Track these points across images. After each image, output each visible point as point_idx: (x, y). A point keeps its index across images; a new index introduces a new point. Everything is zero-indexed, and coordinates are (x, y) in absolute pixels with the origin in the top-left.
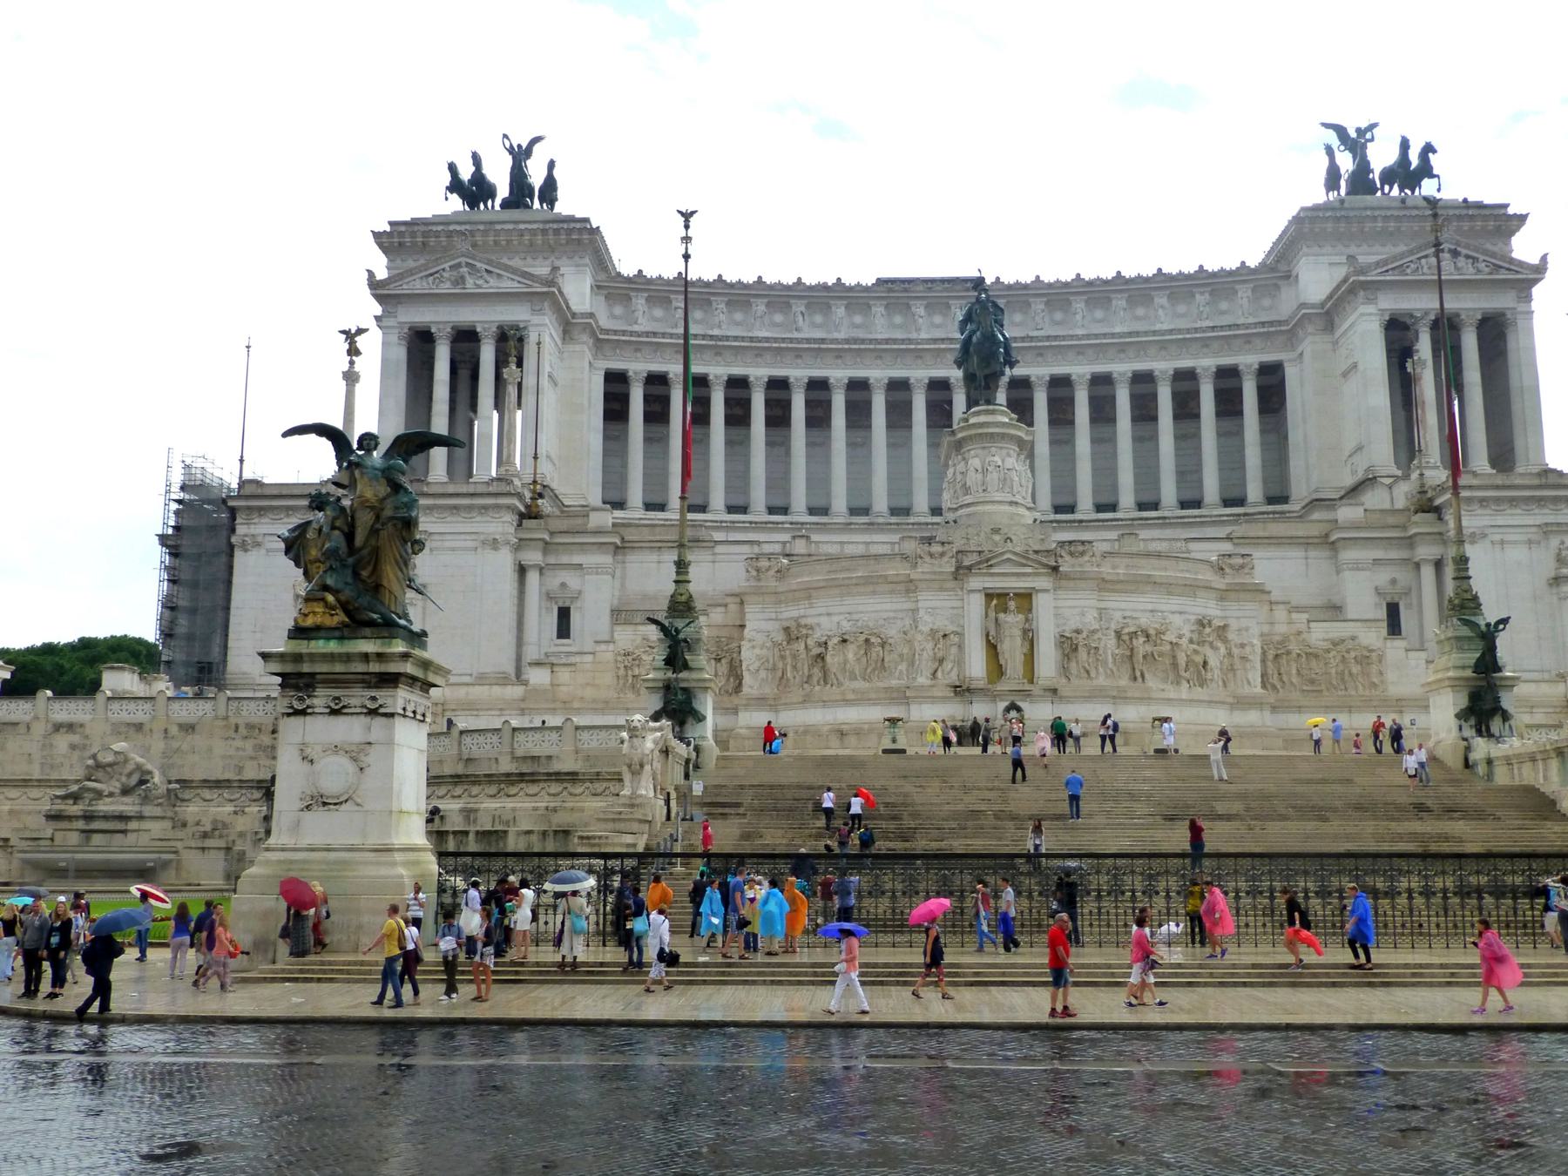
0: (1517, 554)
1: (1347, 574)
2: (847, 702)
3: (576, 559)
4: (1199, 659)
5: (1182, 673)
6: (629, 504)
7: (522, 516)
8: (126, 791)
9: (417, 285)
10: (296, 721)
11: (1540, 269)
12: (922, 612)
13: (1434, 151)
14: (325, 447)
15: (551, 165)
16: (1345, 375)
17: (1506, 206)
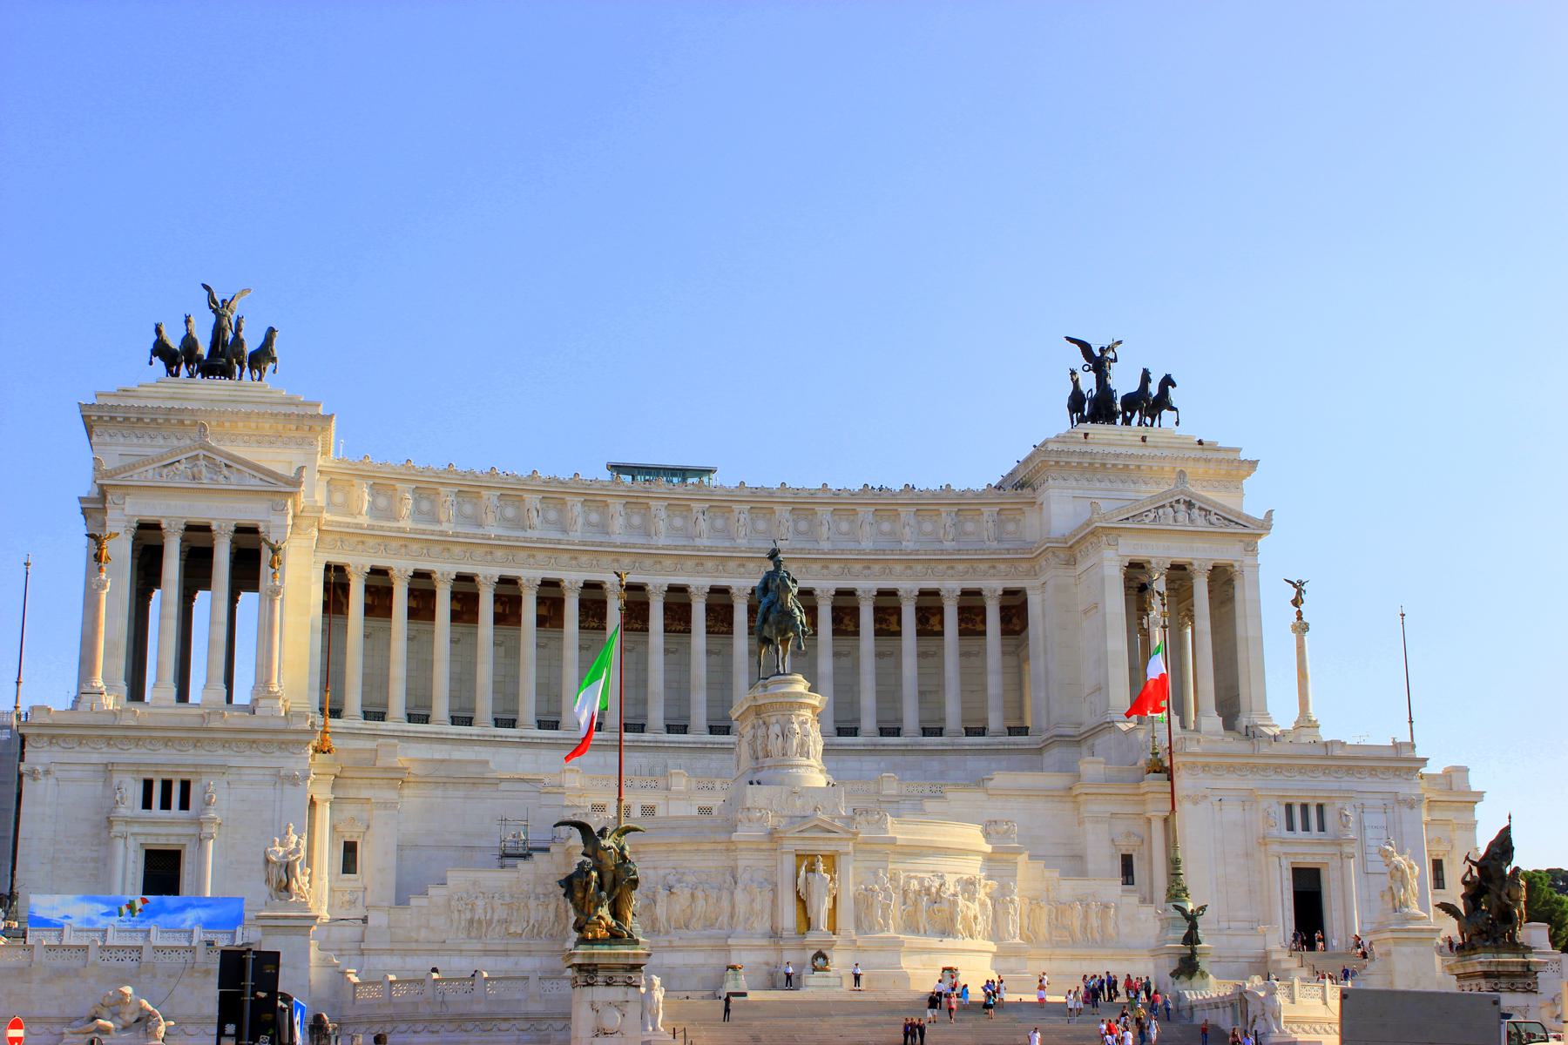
0: (1233, 812)
1: (1089, 826)
2: (672, 948)
3: (365, 794)
4: (971, 914)
5: (960, 927)
6: (346, 712)
7: (316, 750)
8: (125, 1028)
9: (148, 475)
10: (589, 989)
11: (1265, 525)
12: (740, 870)
13: (1174, 385)
14: (576, 832)
15: (271, 331)
16: (1085, 612)
17: (1238, 450)
